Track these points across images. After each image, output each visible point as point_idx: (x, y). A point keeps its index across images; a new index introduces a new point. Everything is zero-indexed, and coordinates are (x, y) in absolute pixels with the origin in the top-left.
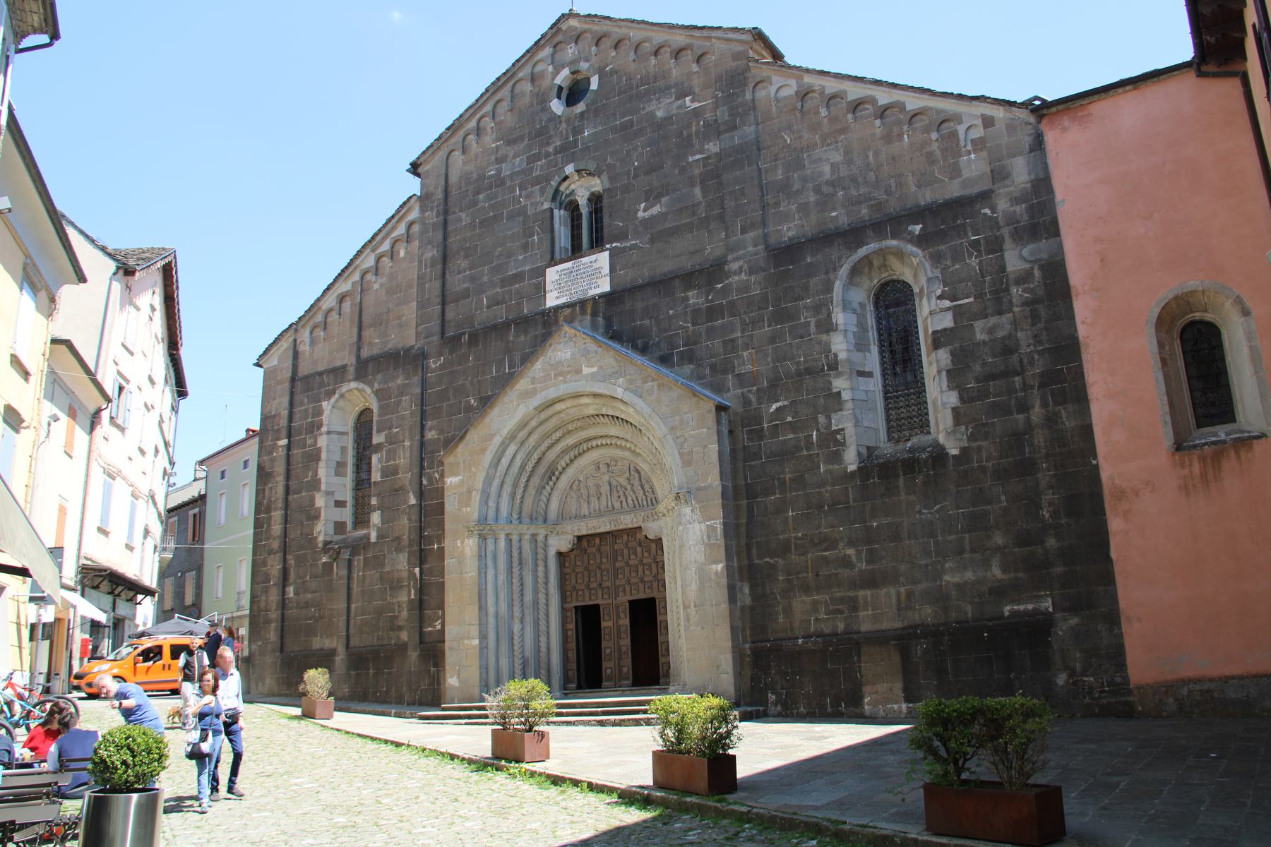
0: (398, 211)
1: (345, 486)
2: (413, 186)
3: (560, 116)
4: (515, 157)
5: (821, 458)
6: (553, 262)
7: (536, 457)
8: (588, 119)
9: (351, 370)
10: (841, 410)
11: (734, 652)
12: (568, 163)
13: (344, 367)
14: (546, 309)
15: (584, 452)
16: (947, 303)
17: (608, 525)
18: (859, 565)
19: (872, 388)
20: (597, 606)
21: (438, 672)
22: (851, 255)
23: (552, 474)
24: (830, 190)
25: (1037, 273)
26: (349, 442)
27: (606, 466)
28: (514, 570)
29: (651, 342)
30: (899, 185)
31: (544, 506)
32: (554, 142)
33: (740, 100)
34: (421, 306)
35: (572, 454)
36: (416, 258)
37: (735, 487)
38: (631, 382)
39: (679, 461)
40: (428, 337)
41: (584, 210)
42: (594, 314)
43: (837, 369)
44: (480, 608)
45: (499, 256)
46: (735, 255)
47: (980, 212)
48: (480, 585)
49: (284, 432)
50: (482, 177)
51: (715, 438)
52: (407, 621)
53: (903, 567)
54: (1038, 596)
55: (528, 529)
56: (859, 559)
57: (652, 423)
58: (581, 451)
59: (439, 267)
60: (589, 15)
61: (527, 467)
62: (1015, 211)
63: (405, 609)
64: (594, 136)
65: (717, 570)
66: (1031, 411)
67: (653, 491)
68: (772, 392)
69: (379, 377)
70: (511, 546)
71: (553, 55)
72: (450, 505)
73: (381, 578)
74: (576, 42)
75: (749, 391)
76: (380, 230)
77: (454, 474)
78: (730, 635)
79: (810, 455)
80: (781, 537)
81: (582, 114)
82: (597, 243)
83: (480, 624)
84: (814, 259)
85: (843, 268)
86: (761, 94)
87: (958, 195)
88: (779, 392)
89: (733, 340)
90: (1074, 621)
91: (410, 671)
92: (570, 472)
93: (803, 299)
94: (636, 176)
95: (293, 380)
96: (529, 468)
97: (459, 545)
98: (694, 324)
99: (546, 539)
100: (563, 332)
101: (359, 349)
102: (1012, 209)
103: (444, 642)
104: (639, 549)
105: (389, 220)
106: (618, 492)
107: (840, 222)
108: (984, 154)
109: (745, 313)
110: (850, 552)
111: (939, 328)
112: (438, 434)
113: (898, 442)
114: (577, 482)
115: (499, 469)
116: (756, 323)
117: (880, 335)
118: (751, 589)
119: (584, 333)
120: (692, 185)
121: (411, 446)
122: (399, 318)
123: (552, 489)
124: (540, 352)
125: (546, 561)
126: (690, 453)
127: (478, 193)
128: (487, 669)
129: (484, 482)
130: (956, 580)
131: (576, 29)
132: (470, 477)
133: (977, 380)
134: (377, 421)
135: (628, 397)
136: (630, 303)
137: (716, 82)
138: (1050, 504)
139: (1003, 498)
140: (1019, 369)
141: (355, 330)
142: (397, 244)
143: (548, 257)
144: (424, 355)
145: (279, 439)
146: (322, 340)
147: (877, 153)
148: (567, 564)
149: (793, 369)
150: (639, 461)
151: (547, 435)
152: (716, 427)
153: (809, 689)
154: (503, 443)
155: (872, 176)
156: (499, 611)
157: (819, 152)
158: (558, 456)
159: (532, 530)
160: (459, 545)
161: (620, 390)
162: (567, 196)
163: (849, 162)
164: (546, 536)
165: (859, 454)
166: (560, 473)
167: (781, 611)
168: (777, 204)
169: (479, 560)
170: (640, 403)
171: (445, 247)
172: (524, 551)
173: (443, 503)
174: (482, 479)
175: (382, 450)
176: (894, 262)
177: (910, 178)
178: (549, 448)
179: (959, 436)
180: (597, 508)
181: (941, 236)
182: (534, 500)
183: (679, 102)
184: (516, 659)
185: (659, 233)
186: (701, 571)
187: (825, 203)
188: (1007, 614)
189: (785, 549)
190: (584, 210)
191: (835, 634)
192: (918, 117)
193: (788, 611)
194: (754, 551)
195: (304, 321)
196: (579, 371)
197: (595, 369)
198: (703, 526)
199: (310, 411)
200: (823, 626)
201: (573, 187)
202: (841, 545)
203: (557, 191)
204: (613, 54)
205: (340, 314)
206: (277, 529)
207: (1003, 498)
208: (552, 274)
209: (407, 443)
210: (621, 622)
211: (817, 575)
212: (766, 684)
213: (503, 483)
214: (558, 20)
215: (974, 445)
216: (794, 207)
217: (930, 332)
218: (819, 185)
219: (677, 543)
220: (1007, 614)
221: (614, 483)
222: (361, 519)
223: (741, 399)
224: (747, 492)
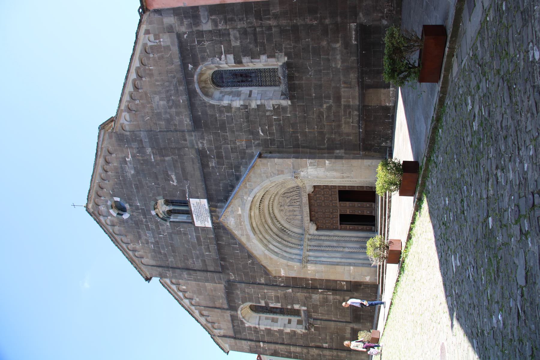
0: (166, 288)
1: (282, 319)
2: (156, 280)
3: (130, 215)
4: (146, 236)
5: (284, 115)
6: (193, 223)
7: (275, 236)
8: (132, 203)
9: (233, 313)
10: (265, 105)
11: (363, 159)
12: (151, 213)
13: (231, 316)
14: (212, 227)
15: (274, 216)
16: (223, 56)
17: (306, 208)
18: (331, 103)
19: (256, 91)
20: (340, 215)
21: (364, 284)
22: (199, 95)
23: (283, 230)
24: (171, 102)
25: (213, 17)
26: (264, 316)
27: (281, 207)
28: (323, 249)
29: (230, 184)
30: (171, 72)
31: (296, 235)
32: (141, 218)
33: (129, 137)
34: (207, 281)
35: (275, 221)
36: (187, 281)
37: (294, 153)
38: (246, 193)
39: (281, 176)
40: (221, 279)
41: (172, 208)
42: (216, 207)
43: (247, 105)
44: (337, 265)
45: (188, 246)
46: (195, 145)
47: (185, 39)
48: (328, 264)
49: (257, 344)
50: (154, 251)
51: (272, 159)
52: (341, 296)
53: (333, 85)
54: (349, 29)
55: (305, 242)
56: (328, 102)
57: (264, 186)
58: (274, 217)
59: (191, 272)
60: (88, 199)
61: (279, 240)
62: (186, 24)
63: (336, 297)
64: (140, 201)
65: (329, 163)
66: (272, 25)
67: (293, 188)
68: (254, 134)
69: (236, 301)
70: (312, 250)
71: (104, 216)
72: (293, 274)
73: (322, 306)
74: (99, 206)
75: (254, 143)
76: (174, 296)
77: (280, 272)
78: (356, 160)
79: (283, 120)
80: (316, 135)
81: (130, 205)
82: (186, 204)
83: (344, 265)
84: (200, 111)
85: (205, 99)
86: (127, 128)
87: (177, 48)
88: (255, 131)
89: (232, 149)
90: (361, 15)
91: (362, 296)
92: (283, 222)
93: (216, 117)
94: (158, 184)
95: (235, 338)
96: (280, 240)
97: (310, 272)
98: (224, 165)
99: (311, 235)
100: (223, 221)
101: (224, 309)
102: (185, 25)
103: (351, 281)
104: (317, 196)
105: (170, 292)
106: (293, 202)
107: (185, 99)
108: (161, 35)
109: (220, 142)
110: (325, 106)
111: (233, 61)
112: (263, 277)
113: (280, 82)
114: (287, 220)
115: (279, 252)
116: (225, 139)
117: (234, 86)
118: (337, 149)
119: (224, 212)
120: (164, 161)
121: (267, 289)
122: (212, 290)
123: (289, 231)
124: (231, 231)
125: (320, 236)
126: (278, 171)
127: (161, 253)
128: (363, 264)
129: (284, 259)
130: (340, 63)
131: (93, 205)
132: (281, 265)
133: (256, 46)
134: (255, 303)
135: (252, 195)
136: (213, 191)
137: (121, 147)
138: (311, 20)
139: (307, 40)
140: (253, 28)
141: (216, 310)
142: (180, 289)
143: (190, 225)
144: (229, 282)
145: (260, 346)
146: (219, 324)
147: (157, 81)
148: (322, 226)
149: (246, 124)
150: (280, 193)
151: (266, 231)
152: (268, 159)
153: (381, 128)
154: (268, 250)
155: (166, 84)
156: (339, 257)
157: (154, 105)
158: (275, 227)
159: (306, 240)
160: (310, 272)
161: (249, 198)
162: (165, 215)
163: (160, 93)
164: (309, 234)
165: (284, 99)
166: (283, 226)
167: (348, 138)
168: (175, 125)
169: (317, 264)
170: (255, 190)
171: (183, 269)
172: (315, 244)
173: (292, 278)
174: (283, 260)
175: (268, 302)
176: (204, 77)
177: (169, 67)
179: (279, 56)
180: (299, 212)
181: (194, 56)
182: (293, 238)
183: (128, 163)
184: (360, 251)
185: (184, 176)
186: (328, 170)
187: (176, 105)
188: (356, 43)
189: (322, 133)
190: (172, 208)
191: (359, 116)
192: (143, 62)
193: (348, 135)
194: (322, 147)
195: (210, 332)
196: (240, 215)
197: (240, 208)
198: (309, 168)
199: (249, 331)
200: (355, 120)
201: (161, 212)
202: (322, 110)
203: (162, 219)
204: (105, 190)
205: (208, 316)
206: (298, 349)
207: (307, 40)
208: (198, 224)
209: (266, 291)
210: (348, 206)
211: (334, 121)
212: (378, 146)
213: (285, 251)
214: (89, 212)
215: (284, 50)
216: (177, 118)
217: (235, 65)
218: (168, 106)
219: (316, 179)
220: (356, 43)
221: (289, 204)
222: (296, 313)
223: (257, 147)
224: (296, 148)
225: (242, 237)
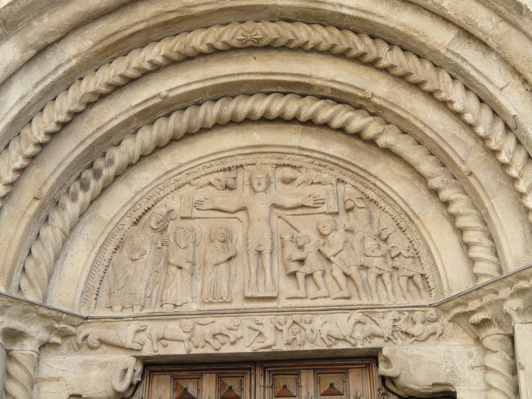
67: (416, 257)
158: (126, 124)
166: (117, 177)
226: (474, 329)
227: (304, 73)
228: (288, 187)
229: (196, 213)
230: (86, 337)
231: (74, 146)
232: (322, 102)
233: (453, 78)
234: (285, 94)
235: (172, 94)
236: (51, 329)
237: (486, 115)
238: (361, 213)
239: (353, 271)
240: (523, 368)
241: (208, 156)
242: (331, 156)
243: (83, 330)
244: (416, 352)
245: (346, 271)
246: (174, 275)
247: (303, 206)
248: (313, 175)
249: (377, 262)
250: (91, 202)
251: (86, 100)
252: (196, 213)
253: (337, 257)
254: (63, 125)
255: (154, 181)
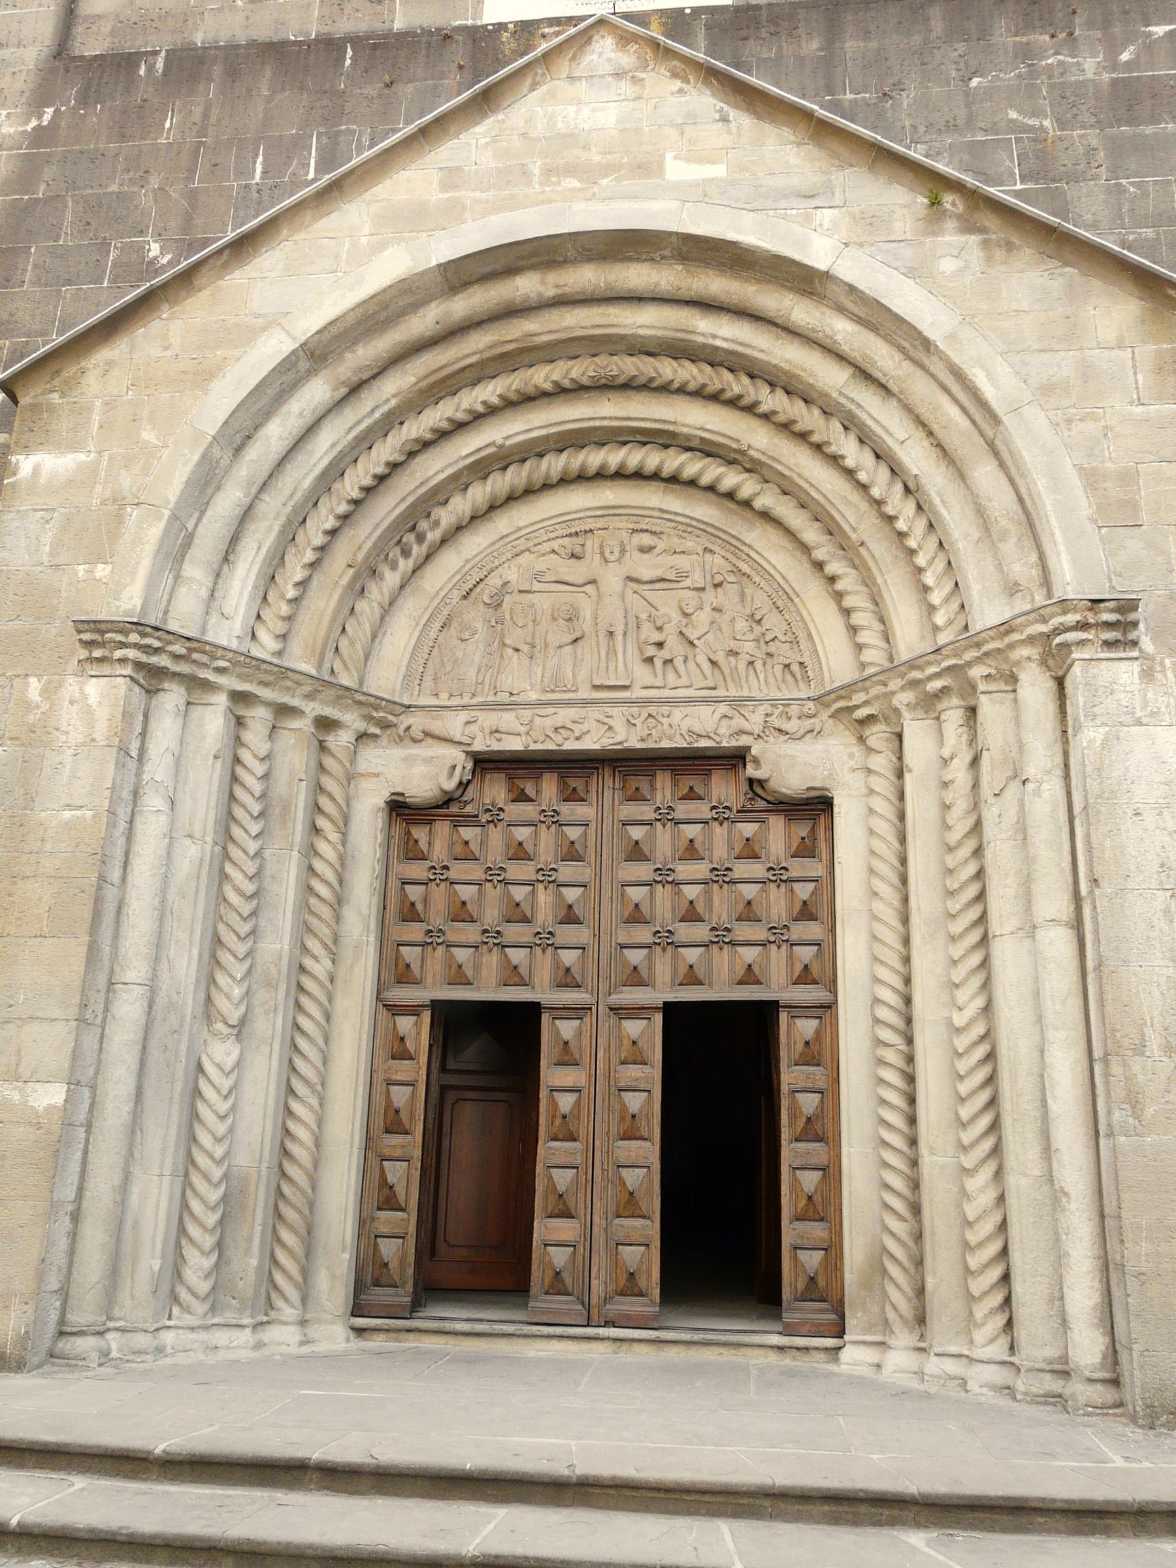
35: (501, 482)
67: (795, 642)
92: (475, 543)
96: (351, 485)
126: (1127, 477)
156: (165, 984)
158: (454, 477)
166: (443, 541)
169: (120, 766)
178: (442, 435)
225: (436, 176)
226: (857, 725)
227: (667, 418)
228: (646, 556)
229: (537, 586)
230: (408, 728)
231: (393, 505)
232: (689, 454)
233: (846, 428)
234: (644, 444)
235: (508, 443)
236: (369, 718)
237: (883, 473)
238: (732, 590)
239: (720, 657)
240: (910, 771)
241: (552, 517)
242: (698, 521)
243: (406, 720)
244: (790, 752)
245: (712, 657)
246: (510, 660)
247: (663, 580)
248: (676, 543)
249: (749, 647)
250: (414, 571)
251: (408, 448)
252: (537, 586)
253: (702, 640)
254: (381, 479)
255: (488, 547)
